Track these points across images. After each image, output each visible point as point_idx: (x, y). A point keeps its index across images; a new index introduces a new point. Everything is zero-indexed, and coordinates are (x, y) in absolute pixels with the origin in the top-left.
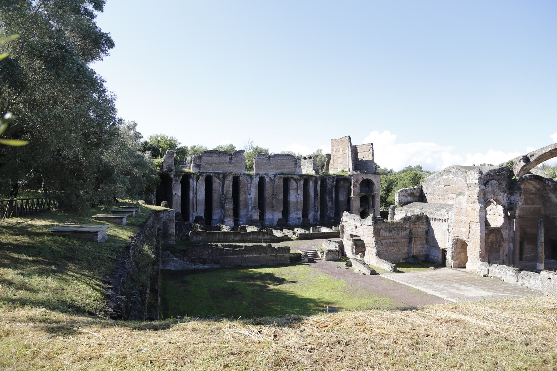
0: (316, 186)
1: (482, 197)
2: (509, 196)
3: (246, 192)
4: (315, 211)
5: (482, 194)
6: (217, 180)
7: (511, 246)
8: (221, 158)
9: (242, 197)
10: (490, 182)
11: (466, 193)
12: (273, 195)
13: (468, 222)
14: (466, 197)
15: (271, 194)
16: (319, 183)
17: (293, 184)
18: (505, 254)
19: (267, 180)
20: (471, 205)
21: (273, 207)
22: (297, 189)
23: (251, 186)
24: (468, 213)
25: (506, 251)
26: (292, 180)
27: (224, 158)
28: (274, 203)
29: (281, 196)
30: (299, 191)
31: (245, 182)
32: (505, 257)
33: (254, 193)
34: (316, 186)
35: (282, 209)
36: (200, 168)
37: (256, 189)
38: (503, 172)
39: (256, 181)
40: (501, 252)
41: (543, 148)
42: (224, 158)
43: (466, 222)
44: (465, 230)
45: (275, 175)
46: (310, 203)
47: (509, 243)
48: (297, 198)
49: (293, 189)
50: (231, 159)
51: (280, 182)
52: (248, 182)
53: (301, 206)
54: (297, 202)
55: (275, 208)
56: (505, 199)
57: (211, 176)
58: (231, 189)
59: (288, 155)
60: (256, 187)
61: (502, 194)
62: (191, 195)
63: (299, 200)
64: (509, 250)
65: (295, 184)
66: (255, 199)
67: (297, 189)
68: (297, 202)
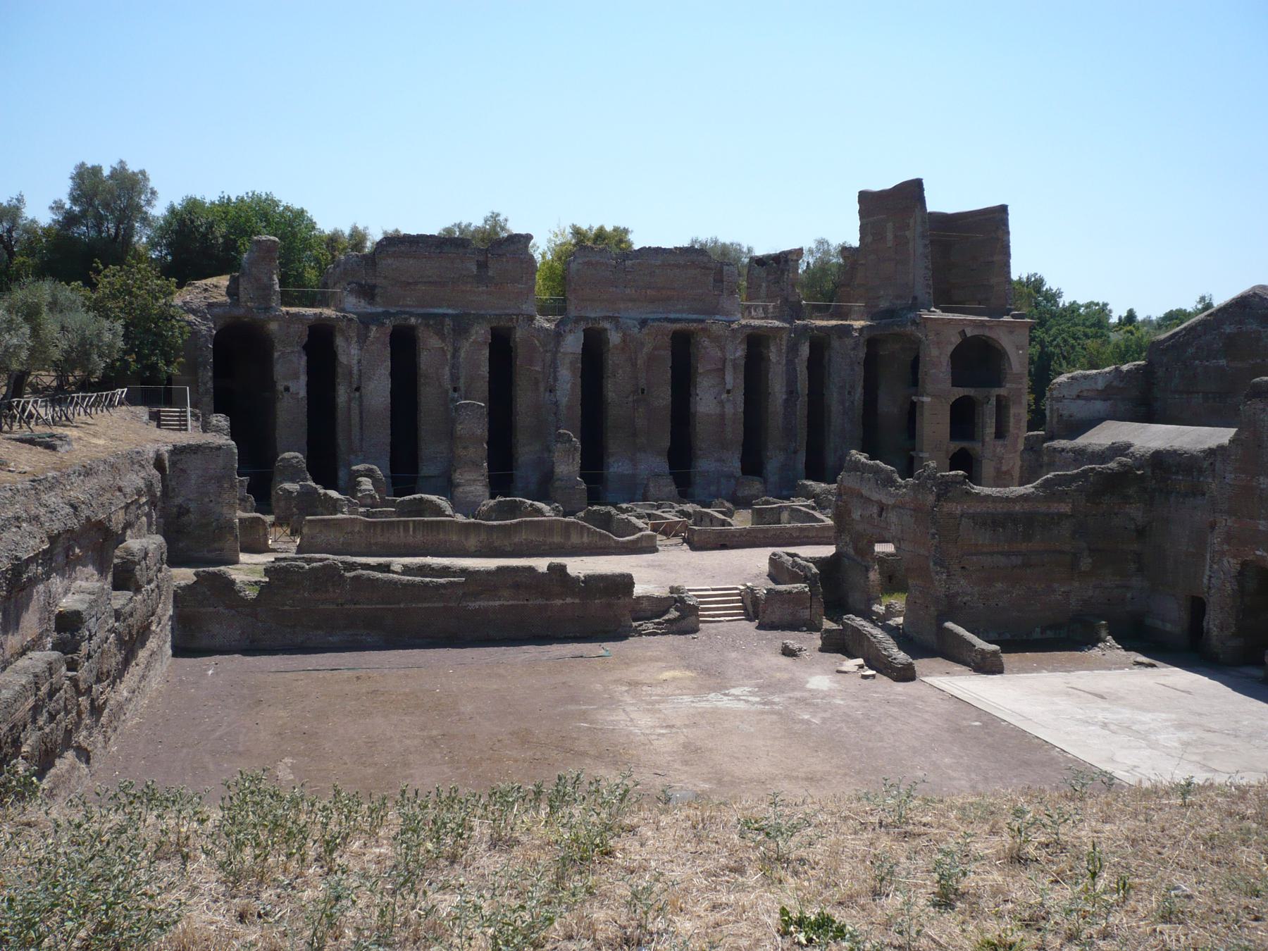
0: (790, 363)
9: (524, 400)
16: (805, 350)
19: (614, 338)
23: (554, 361)
29: (663, 397)
35: (666, 443)
48: (721, 403)
50: (482, 266)
53: (735, 432)
54: (722, 416)
57: (413, 329)
58: (485, 370)
62: (342, 394)
63: (729, 409)
68: (722, 416)
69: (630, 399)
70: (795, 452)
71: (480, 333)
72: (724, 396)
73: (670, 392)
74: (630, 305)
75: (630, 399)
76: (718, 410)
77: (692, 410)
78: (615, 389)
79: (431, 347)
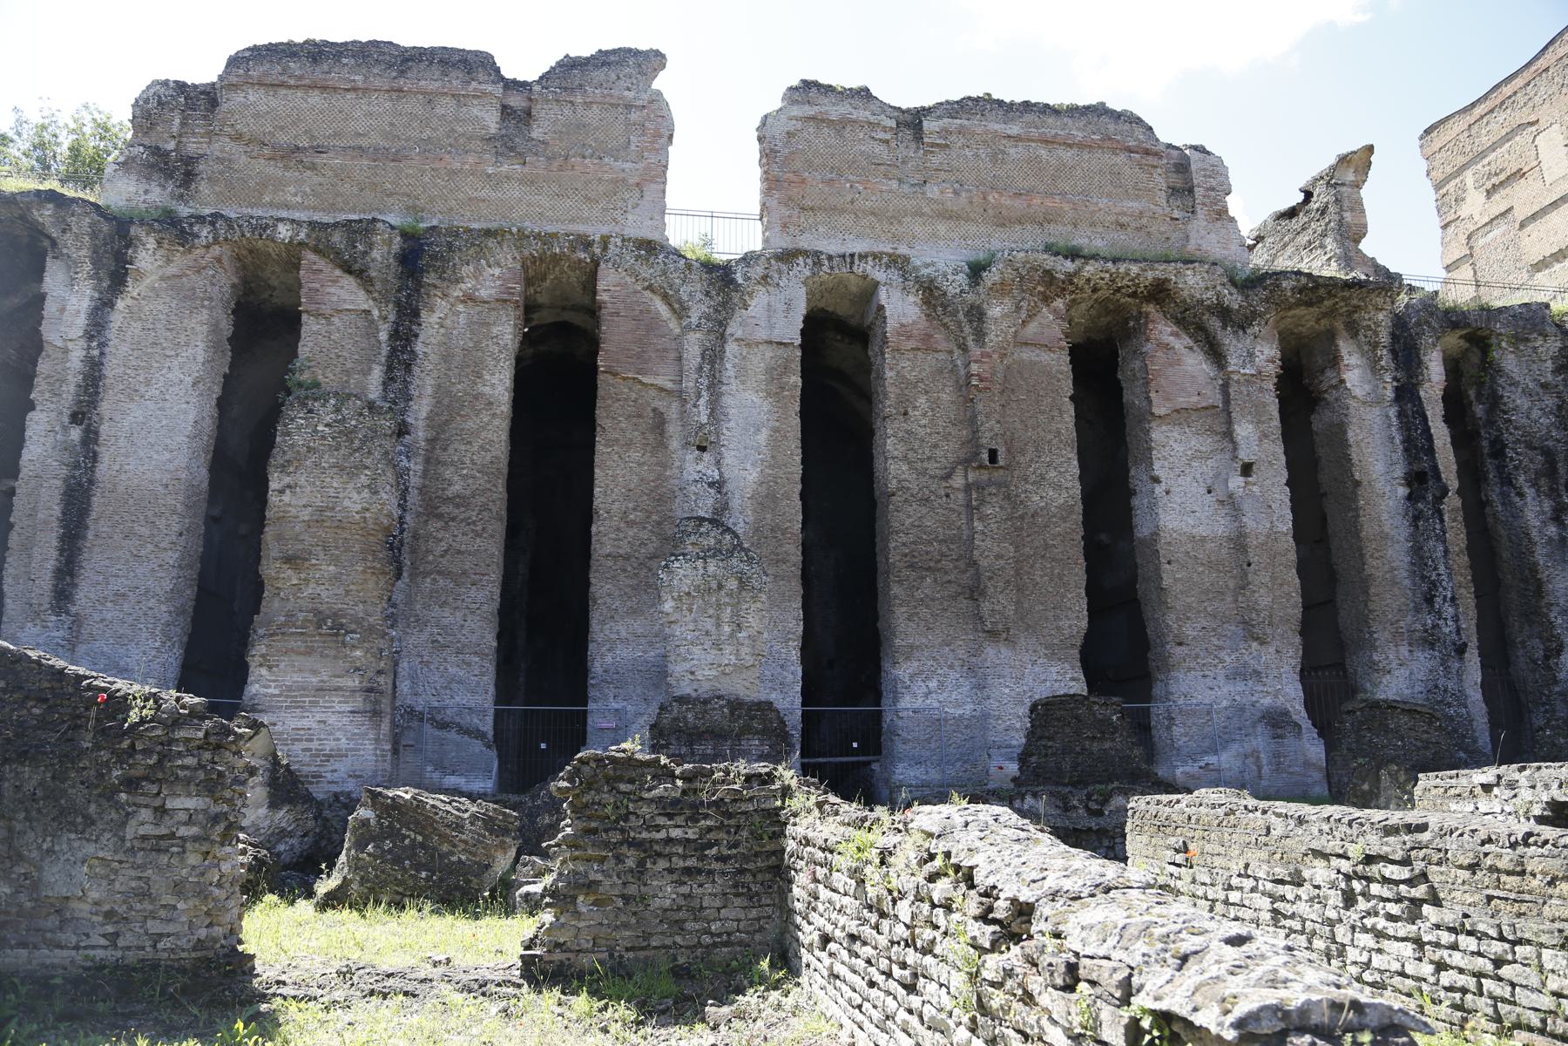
0: (1407, 394)
3: (659, 423)
4: (1429, 640)
6: (347, 293)
8: (413, 105)
9: (616, 474)
12: (966, 462)
15: (950, 450)
17: (1174, 368)
19: (900, 308)
21: (975, 592)
22: (1221, 420)
23: (713, 356)
26: (1163, 331)
27: (446, 107)
28: (991, 549)
29: (1057, 482)
30: (1244, 430)
31: (652, 324)
33: (752, 442)
34: (1407, 394)
36: (189, 177)
37: (774, 391)
39: (776, 315)
42: (446, 107)
45: (976, 270)
46: (1374, 566)
49: (1181, 416)
51: (1039, 346)
52: (680, 311)
53: (1278, 590)
54: (1239, 542)
55: (998, 603)
59: (1099, 110)
60: (775, 374)
65: (1195, 364)
66: (767, 499)
67: (1221, 420)
68: (1239, 542)
69: (958, 481)
70: (1461, 650)
71: (492, 276)
72: (1236, 482)
73: (1074, 468)
74: (942, 228)
75: (958, 481)
76: (1220, 526)
77: (1143, 530)
78: (911, 444)
79: (338, 322)
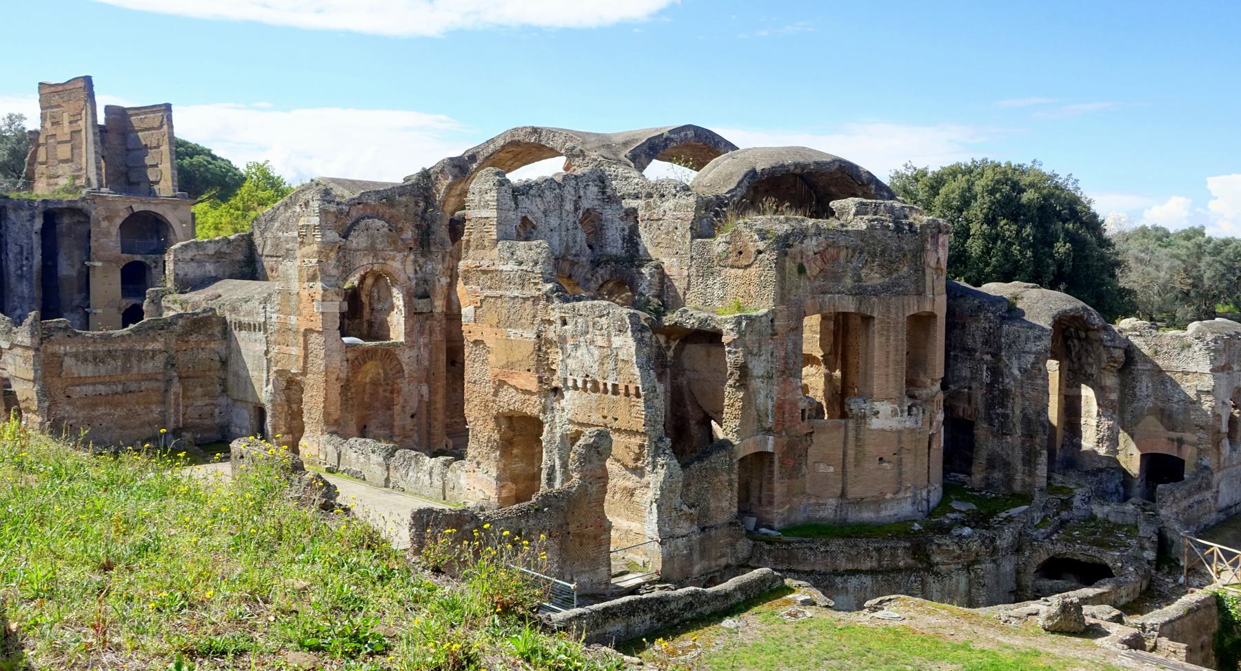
1: (333, 262)
2: (421, 261)
5: (333, 255)
7: (425, 389)
10: (362, 223)
11: (298, 254)
13: (302, 330)
14: (298, 262)
18: (409, 412)
20: (306, 285)
24: (301, 306)
25: (414, 403)
32: (409, 421)
38: (404, 199)
40: (397, 408)
41: (493, 141)
43: (297, 332)
44: (296, 351)
47: (420, 382)
56: (410, 270)
61: (399, 256)
64: (420, 401)
